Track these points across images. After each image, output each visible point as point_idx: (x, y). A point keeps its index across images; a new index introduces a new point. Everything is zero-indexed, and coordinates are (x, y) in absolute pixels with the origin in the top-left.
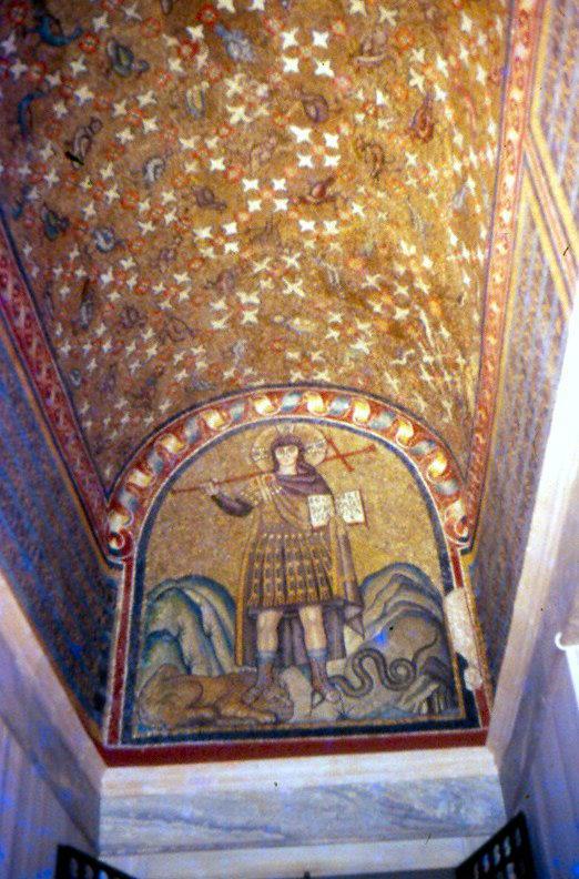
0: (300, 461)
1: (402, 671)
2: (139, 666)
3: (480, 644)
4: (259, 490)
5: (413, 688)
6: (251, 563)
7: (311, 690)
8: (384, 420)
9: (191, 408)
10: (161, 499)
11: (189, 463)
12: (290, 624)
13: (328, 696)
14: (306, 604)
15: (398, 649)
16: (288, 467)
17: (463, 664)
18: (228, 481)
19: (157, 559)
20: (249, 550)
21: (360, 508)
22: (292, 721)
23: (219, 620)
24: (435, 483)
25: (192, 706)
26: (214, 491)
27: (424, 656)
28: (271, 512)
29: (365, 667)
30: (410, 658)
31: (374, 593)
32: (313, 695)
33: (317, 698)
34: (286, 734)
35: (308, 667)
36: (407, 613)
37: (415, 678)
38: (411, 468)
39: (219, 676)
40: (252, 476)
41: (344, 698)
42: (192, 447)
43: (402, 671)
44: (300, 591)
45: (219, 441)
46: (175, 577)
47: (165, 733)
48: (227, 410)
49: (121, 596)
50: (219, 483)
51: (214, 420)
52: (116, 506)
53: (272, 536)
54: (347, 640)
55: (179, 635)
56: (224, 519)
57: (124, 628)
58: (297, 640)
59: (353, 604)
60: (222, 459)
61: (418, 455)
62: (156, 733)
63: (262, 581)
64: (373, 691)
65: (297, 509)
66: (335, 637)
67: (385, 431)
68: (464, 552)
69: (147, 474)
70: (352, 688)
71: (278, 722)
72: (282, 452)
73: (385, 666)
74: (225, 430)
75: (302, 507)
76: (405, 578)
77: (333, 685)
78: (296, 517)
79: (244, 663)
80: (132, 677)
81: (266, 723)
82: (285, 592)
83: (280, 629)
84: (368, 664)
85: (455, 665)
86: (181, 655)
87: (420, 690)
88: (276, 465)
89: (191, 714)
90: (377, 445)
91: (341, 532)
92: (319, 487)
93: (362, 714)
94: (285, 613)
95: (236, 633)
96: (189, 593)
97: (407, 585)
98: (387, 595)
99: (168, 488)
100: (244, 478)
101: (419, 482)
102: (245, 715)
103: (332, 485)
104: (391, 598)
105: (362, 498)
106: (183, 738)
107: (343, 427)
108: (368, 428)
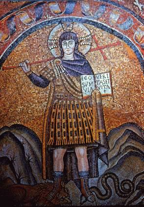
0: (76, 49)
13: (89, 199)
15: (126, 174)
16: (69, 57)
21: (109, 85)
23: (34, 153)
31: (115, 140)
32: (81, 197)
35: (78, 183)
36: (131, 154)
58: (74, 167)
59: (103, 146)
63: (55, 130)
73: (119, 183)
76: (132, 132)
79: (47, 178)
82: (68, 137)
84: (110, 181)
88: (63, 53)
94: (68, 150)
98: (122, 142)
104: (123, 144)
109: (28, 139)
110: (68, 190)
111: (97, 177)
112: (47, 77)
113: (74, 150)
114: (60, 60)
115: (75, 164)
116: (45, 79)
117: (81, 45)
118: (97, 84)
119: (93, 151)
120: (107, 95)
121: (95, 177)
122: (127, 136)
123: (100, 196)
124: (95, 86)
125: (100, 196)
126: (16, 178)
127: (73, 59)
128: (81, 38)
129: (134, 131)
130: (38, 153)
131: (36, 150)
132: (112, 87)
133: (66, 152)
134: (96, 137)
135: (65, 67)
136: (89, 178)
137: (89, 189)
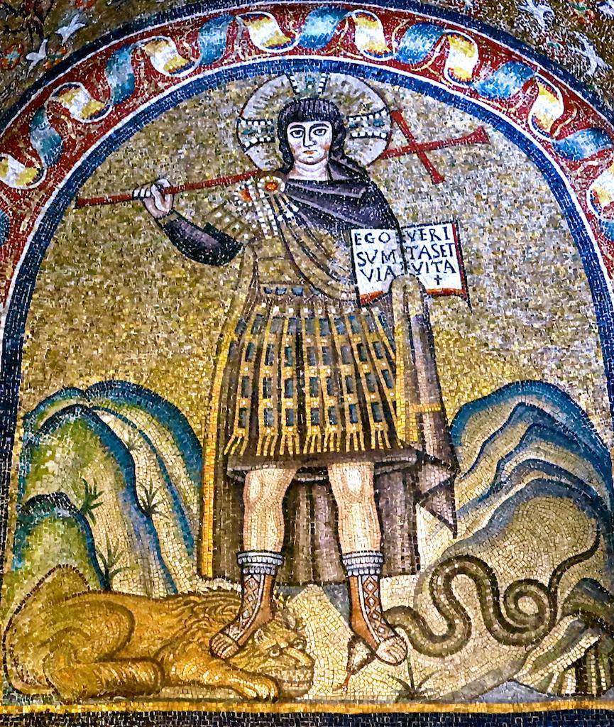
0: (336, 148)
1: (528, 606)
4: (252, 209)
5: (549, 643)
6: (234, 362)
7: (349, 634)
8: (508, 81)
9: (118, 34)
10: (55, 215)
11: (112, 144)
12: (310, 498)
13: (381, 652)
14: (344, 456)
15: (522, 558)
16: (312, 171)
18: (190, 187)
19: (47, 346)
20: (231, 336)
21: (454, 261)
22: (309, 696)
23: (168, 481)
24: (602, 217)
25: (109, 658)
26: (161, 207)
27: (572, 577)
28: (276, 257)
29: (455, 593)
30: (545, 581)
31: (479, 440)
32: (351, 645)
33: (361, 652)
36: (540, 488)
37: (553, 624)
39: (168, 598)
40: (238, 179)
41: (412, 652)
42: (121, 108)
44: (331, 429)
45: (174, 100)
46: (81, 384)
48: (193, 37)
50: (173, 191)
51: (164, 56)
54: (421, 535)
55: (87, 507)
56: (181, 267)
59: (436, 462)
60: (180, 137)
61: (571, 157)
63: (255, 402)
64: (470, 644)
65: (328, 255)
66: (398, 529)
67: (506, 102)
69: (30, 164)
70: (431, 637)
71: (282, 697)
72: (300, 132)
73: (496, 593)
74: (187, 78)
75: (340, 255)
76: (542, 413)
77: (392, 627)
78: (326, 270)
81: (258, 699)
82: (302, 430)
83: (289, 507)
84: (463, 587)
86: (92, 549)
87: (563, 648)
88: (289, 159)
89: (110, 672)
90: (490, 130)
91: (415, 310)
92: (372, 212)
93: (447, 690)
95: (202, 509)
96: (107, 419)
97: (543, 428)
98: (504, 448)
99: (69, 193)
100: (223, 182)
101: (571, 213)
102: (217, 679)
103: (398, 208)
104: (510, 455)
105: (457, 239)
107: (421, 88)
108: (474, 94)
109: (152, 433)
110: (298, 621)
111: (413, 573)
112: (229, 233)
113: (326, 473)
114: (279, 180)
116: (222, 238)
117: (352, 138)
118: (408, 257)
119: (397, 478)
120: (447, 293)
121: (404, 573)
122: (521, 428)
123: (421, 640)
124: (405, 266)
125: (421, 640)
126: (99, 571)
127: (325, 178)
128: (354, 117)
129: (547, 410)
130: (185, 484)
131: (178, 469)
132: (462, 269)
133: (293, 480)
134: (407, 429)
135: (296, 203)
136: (380, 577)
137: (383, 615)
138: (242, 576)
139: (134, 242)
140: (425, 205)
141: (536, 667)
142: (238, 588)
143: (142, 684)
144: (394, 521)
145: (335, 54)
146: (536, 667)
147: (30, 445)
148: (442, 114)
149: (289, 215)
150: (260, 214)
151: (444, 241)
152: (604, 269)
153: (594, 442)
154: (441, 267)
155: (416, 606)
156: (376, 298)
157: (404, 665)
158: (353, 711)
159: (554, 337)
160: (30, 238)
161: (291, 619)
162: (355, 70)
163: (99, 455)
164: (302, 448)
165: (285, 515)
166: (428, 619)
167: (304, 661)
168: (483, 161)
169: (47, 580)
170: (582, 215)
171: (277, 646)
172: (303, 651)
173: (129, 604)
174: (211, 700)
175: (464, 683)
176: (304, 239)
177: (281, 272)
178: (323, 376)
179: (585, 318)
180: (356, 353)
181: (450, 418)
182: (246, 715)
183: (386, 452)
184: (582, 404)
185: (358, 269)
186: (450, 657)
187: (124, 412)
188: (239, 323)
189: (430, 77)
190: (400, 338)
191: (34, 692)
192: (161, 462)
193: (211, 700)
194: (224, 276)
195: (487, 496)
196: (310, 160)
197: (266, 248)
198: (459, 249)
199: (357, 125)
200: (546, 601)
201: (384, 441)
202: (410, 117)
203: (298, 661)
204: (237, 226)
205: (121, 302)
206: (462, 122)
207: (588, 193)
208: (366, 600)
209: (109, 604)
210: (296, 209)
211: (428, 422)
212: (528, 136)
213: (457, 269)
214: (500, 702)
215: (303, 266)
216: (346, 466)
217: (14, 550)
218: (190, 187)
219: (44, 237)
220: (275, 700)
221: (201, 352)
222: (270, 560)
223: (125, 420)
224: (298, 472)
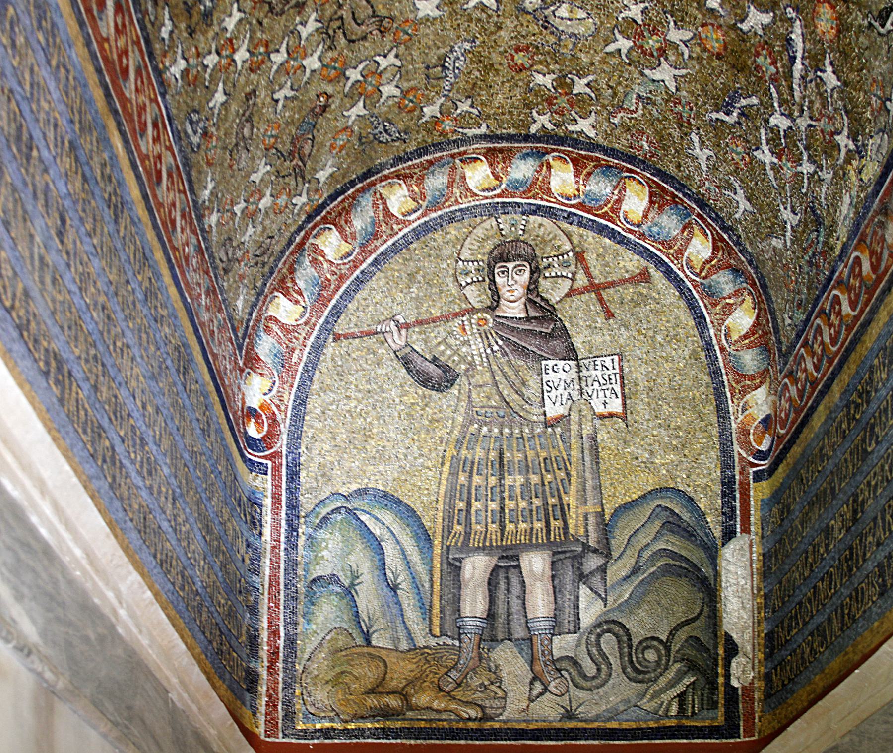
0: (532, 287)
1: (651, 655)
2: (300, 628)
3: (759, 622)
5: (663, 681)
6: (454, 474)
7: (530, 675)
10: (318, 348)
11: (359, 282)
12: (507, 578)
15: (649, 622)
16: (513, 309)
17: (732, 649)
18: (420, 323)
20: (451, 452)
23: (408, 565)
25: (372, 691)
26: (398, 340)
27: (682, 635)
30: (664, 638)
32: (531, 683)
33: (538, 687)
34: (495, 734)
36: (667, 570)
37: (666, 668)
38: (700, 321)
39: (410, 650)
40: (456, 315)
43: (651, 655)
44: (523, 526)
46: (343, 490)
47: (338, 726)
49: (268, 519)
50: (407, 326)
52: (252, 361)
53: (485, 429)
55: (352, 585)
56: (416, 392)
57: (275, 568)
58: (515, 604)
59: (595, 551)
62: (328, 725)
63: (469, 505)
65: (524, 383)
67: (667, 244)
68: (758, 477)
69: (297, 302)
70: (585, 677)
71: (486, 718)
72: (505, 272)
73: (630, 647)
74: (416, 221)
75: (533, 382)
77: (559, 670)
78: (522, 395)
80: (291, 642)
81: (470, 719)
83: (492, 585)
84: (608, 643)
85: (721, 651)
87: (672, 684)
89: (372, 701)
91: (587, 430)
92: (558, 345)
95: (432, 586)
96: (364, 518)
97: (673, 525)
98: (643, 539)
101: (708, 347)
105: (621, 369)
106: (360, 733)
107: (602, 230)
108: (642, 236)
110: (497, 667)
115: (518, 597)
116: (446, 369)
117: (546, 278)
118: (584, 384)
119: (568, 563)
120: (611, 415)
121: (569, 632)
122: (658, 524)
124: (581, 394)
127: (523, 315)
128: (547, 258)
131: (415, 557)
135: (501, 337)
136: (553, 635)
138: (460, 634)
139: (379, 371)
140: (598, 339)
141: (653, 698)
142: (457, 643)
143: (394, 709)
144: (564, 595)
145: (534, 197)
146: (653, 698)
147: (310, 537)
148: (616, 255)
149: (496, 348)
150: (473, 347)
151: (611, 371)
152: (729, 395)
153: (707, 535)
154: (608, 393)
155: (576, 655)
156: (558, 420)
157: (566, 697)
158: (531, 727)
159: (686, 452)
160: (300, 369)
161: (492, 664)
162: (549, 213)
163: (359, 546)
164: (502, 540)
165: (490, 590)
166: (583, 665)
167: (500, 694)
168: (645, 298)
169: (328, 638)
170: (717, 348)
171: (483, 683)
172: (499, 687)
173: (383, 654)
174: (439, 720)
175: (604, 708)
176: (506, 369)
177: (489, 398)
178: (518, 484)
179: (710, 437)
180: (542, 465)
181: (607, 517)
182: (461, 729)
183: (561, 543)
184: (702, 506)
185: (546, 394)
186: (597, 691)
187: (376, 513)
188: (458, 441)
189: (609, 220)
190: (575, 453)
191: (323, 715)
192: (403, 551)
193: (439, 720)
194: (445, 401)
195: (629, 577)
196: (512, 298)
197: (478, 377)
198: (622, 378)
199: (549, 266)
200: (663, 652)
201: (560, 536)
202: (591, 258)
203: (496, 694)
204: (456, 358)
205: (370, 423)
206: (631, 263)
207: (723, 328)
208: (543, 652)
209: (370, 654)
210: (500, 343)
211: (592, 520)
212: (682, 275)
213: (619, 395)
214: (627, 721)
215: (505, 393)
216: (532, 554)
217: (304, 616)
218: (420, 323)
219: (311, 366)
220: (481, 719)
221: (430, 465)
222: (478, 623)
223: (377, 519)
224: (499, 558)
